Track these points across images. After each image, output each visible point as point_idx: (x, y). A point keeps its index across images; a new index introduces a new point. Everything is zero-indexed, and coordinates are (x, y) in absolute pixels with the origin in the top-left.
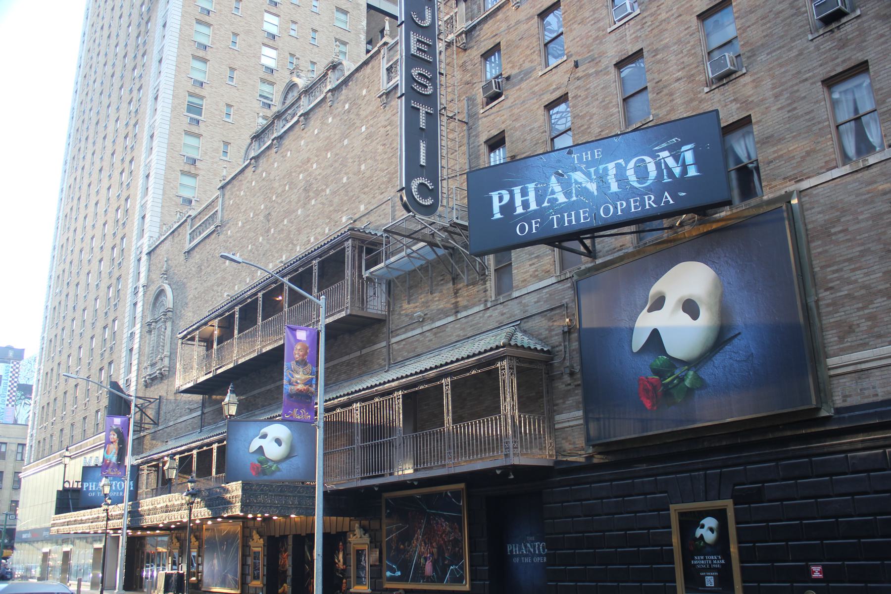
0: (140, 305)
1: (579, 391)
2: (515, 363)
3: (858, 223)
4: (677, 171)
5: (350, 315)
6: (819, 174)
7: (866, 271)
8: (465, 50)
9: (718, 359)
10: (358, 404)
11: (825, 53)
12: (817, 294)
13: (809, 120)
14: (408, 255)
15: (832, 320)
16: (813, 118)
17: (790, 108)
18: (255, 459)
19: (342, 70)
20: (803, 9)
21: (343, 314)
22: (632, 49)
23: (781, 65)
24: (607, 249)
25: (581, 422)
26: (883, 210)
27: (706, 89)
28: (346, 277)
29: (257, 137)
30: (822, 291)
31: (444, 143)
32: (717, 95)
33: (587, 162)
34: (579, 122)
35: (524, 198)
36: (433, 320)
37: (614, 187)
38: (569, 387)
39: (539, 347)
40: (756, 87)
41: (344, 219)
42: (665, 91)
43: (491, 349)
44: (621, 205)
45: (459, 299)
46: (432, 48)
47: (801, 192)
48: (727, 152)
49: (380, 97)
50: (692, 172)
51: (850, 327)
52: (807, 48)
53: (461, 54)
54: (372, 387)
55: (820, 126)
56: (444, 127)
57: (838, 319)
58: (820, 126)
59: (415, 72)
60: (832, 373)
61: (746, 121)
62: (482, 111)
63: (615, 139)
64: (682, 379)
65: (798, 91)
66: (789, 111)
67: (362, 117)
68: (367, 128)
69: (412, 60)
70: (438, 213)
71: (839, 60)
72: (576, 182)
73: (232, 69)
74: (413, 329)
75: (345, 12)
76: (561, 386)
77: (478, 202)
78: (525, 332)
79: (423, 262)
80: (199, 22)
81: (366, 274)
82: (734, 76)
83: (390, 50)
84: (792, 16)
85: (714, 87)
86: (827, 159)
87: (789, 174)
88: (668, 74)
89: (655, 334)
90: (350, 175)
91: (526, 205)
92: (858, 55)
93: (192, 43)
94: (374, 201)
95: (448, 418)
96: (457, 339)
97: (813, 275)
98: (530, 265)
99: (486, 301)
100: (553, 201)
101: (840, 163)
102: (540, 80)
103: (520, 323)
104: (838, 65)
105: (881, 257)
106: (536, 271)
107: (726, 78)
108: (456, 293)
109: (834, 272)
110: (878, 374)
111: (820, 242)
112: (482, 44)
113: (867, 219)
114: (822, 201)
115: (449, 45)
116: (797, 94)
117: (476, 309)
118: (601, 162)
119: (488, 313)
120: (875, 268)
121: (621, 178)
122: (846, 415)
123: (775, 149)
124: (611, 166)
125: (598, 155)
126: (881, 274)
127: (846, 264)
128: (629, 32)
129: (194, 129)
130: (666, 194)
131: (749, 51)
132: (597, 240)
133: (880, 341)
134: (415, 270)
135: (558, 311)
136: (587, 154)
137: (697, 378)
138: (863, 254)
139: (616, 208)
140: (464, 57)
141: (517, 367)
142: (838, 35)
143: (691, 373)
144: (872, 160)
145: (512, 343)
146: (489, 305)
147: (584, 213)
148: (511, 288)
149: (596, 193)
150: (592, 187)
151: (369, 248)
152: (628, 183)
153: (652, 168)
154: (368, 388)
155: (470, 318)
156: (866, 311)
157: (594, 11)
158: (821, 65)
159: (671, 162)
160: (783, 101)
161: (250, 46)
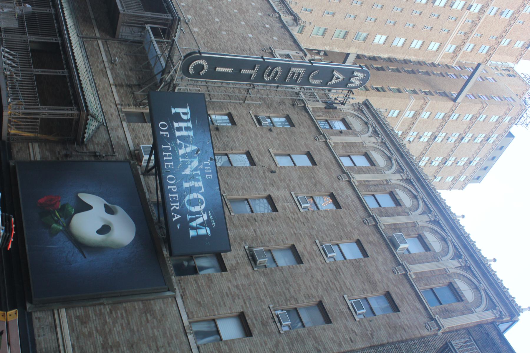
1: (54, 159)
2: (75, 117)
3: (152, 329)
4: (194, 224)
5: (119, 13)
6: (185, 308)
7: (121, 332)
8: (293, 105)
9: (69, 245)
10: (53, 12)
11: (260, 314)
12: (108, 304)
13: (220, 304)
14: (157, 56)
15: (90, 312)
16: (220, 306)
17: (229, 293)
19: (292, 25)
20: (289, 303)
21: (120, 8)
22: (278, 206)
23: (256, 290)
24: (150, 182)
25: (32, 159)
26: (158, 343)
27: (246, 247)
28: (146, 13)
30: (110, 307)
31: (231, 86)
32: (242, 253)
33: (204, 169)
34: (235, 171)
35: (184, 128)
36: (112, 70)
37: (186, 185)
38: (57, 153)
39: (86, 135)
40: (244, 275)
41: (189, 17)
42: (249, 223)
43: (86, 103)
44: (174, 189)
45: (125, 88)
46: (295, 82)
47: (175, 298)
48: (202, 254)
49: (270, 48)
50: (192, 233)
51: (85, 323)
52: (265, 304)
53: (291, 102)
54: (66, 22)
55: (215, 310)
56: (243, 85)
57: (91, 316)
58: (215, 310)
59: (279, 69)
60: (56, 312)
61: (223, 268)
62: (251, 112)
63: (217, 188)
64: (57, 222)
65: (239, 298)
66: (227, 293)
67: (259, 36)
68: (250, 38)
69: (287, 68)
70: (184, 76)
71: (255, 321)
72: (191, 162)
74: (106, 56)
75: (344, 37)
76: (58, 148)
77: (184, 100)
78: (98, 128)
79: (153, 65)
81: (148, 27)
82: (253, 263)
83: (302, 58)
84: (286, 297)
85: (248, 251)
86: (194, 313)
87: (187, 291)
88: (259, 225)
89: (89, 207)
90: (219, 24)
91: (180, 129)
92: (256, 332)
94: (199, 38)
95: (40, 72)
96: (97, 84)
97: (121, 303)
98: (144, 135)
99: (122, 105)
100: (180, 146)
101: (191, 320)
102: (267, 150)
103: (104, 126)
104: (252, 321)
105: (128, 341)
106: (139, 138)
107: (252, 258)
108: (129, 86)
109: (122, 314)
110: (53, 337)
111: (141, 307)
112: (296, 116)
113: (154, 334)
114: (168, 309)
115: (297, 94)
116: (237, 298)
117: (117, 98)
118: (204, 178)
119: (113, 106)
120: (122, 337)
121: (192, 190)
122: (27, 318)
123: (204, 284)
124: (200, 184)
125: (208, 177)
126: (118, 340)
127: (126, 321)
128: (289, 205)
130: (179, 216)
131: (267, 272)
132: (154, 176)
133: (75, 339)
134: (148, 59)
135: (110, 150)
136: (209, 169)
137: (57, 231)
138: (132, 331)
139: (172, 185)
140: (288, 103)
141: (73, 119)
142: (270, 321)
143: (61, 228)
144: (190, 337)
145: (89, 117)
146: (119, 107)
147: (171, 165)
148: (129, 121)
149: (183, 173)
150: (187, 171)
151: (166, 30)
152: (188, 193)
153: (197, 209)
154: (65, 19)
155: (111, 94)
156: (94, 332)
157: (306, 186)
158: (253, 312)
159: (200, 221)
160: (234, 290)
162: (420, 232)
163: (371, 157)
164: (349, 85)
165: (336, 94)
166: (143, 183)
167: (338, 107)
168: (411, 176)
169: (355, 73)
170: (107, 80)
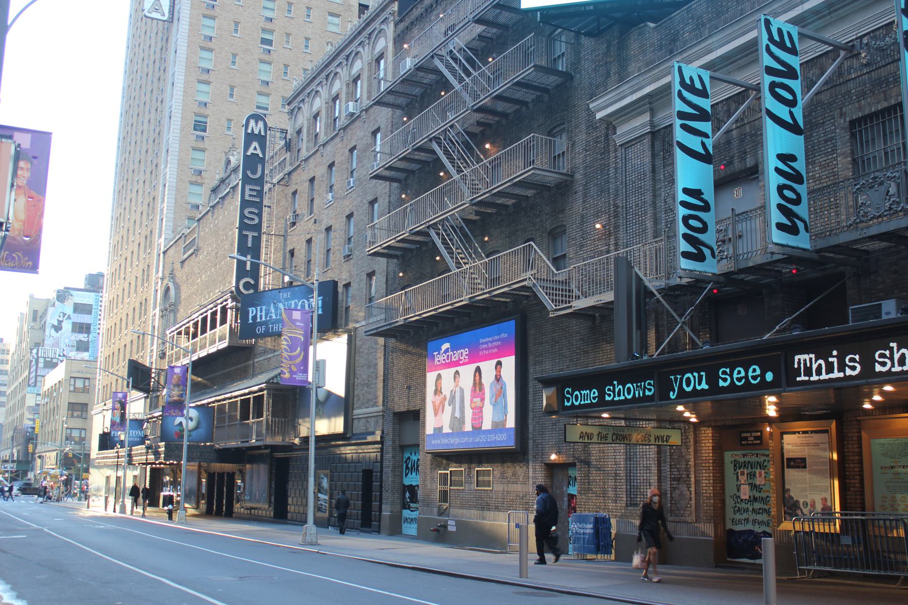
0: (159, 292)
2: (272, 392)
18: (177, 429)
29: (214, 190)
59: (246, 212)
69: (245, 204)
73: (232, 88)
75: (338, 16)
80: (202, 48)
91: (261, 318)
93: (197, 69)
100: (271, 317)
124: (293, 302)
129: (200, 145)
153: (307, 306)
161: (248, 63)
162: (352, 79)
164: (263, 133)
165: (276, 144)
167: (289, 137)
168: (323, 75)
169: (249, 131)
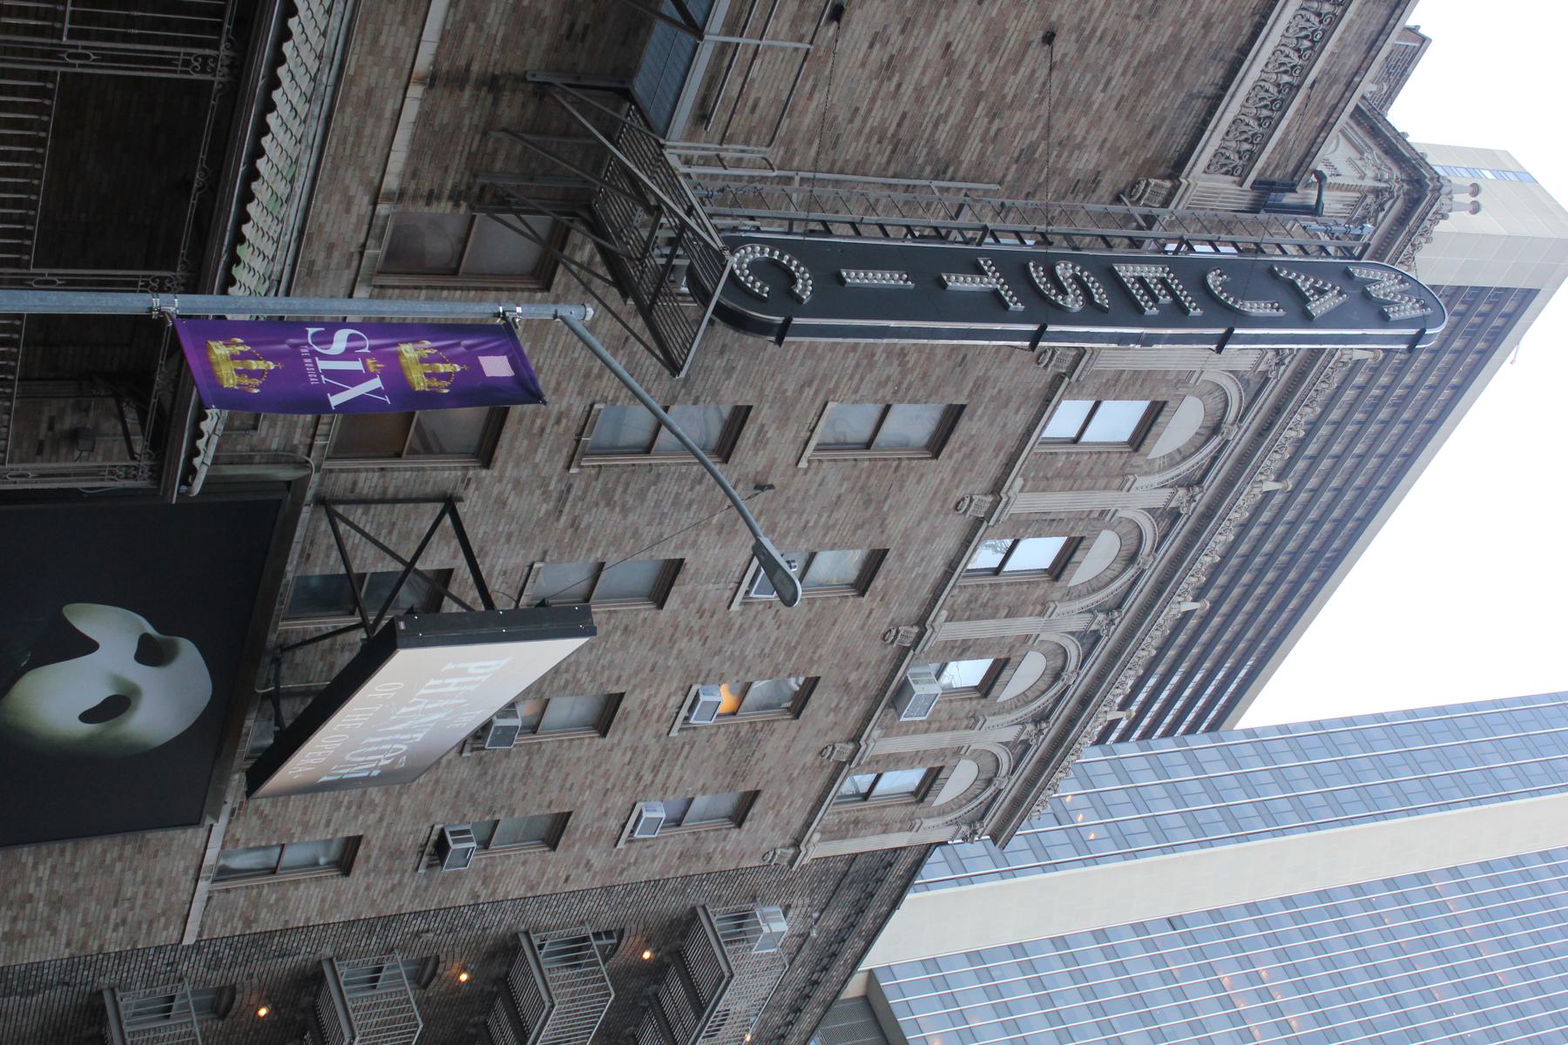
16: (316, 826)
38: (44, 426)
96: (350, 69)
119: (362, 203)
155: (384, 131)
163: (1160, 419)
166: (299, 533)
170: (406, 54)
